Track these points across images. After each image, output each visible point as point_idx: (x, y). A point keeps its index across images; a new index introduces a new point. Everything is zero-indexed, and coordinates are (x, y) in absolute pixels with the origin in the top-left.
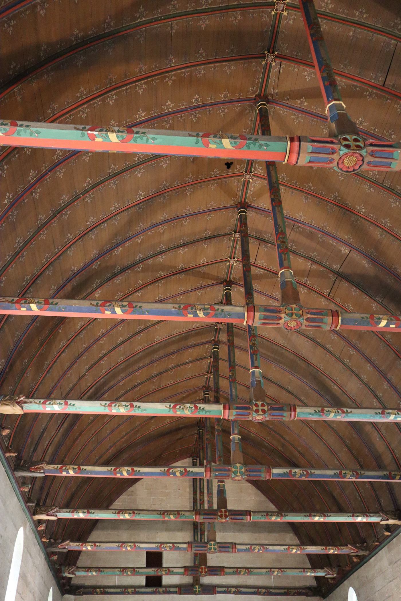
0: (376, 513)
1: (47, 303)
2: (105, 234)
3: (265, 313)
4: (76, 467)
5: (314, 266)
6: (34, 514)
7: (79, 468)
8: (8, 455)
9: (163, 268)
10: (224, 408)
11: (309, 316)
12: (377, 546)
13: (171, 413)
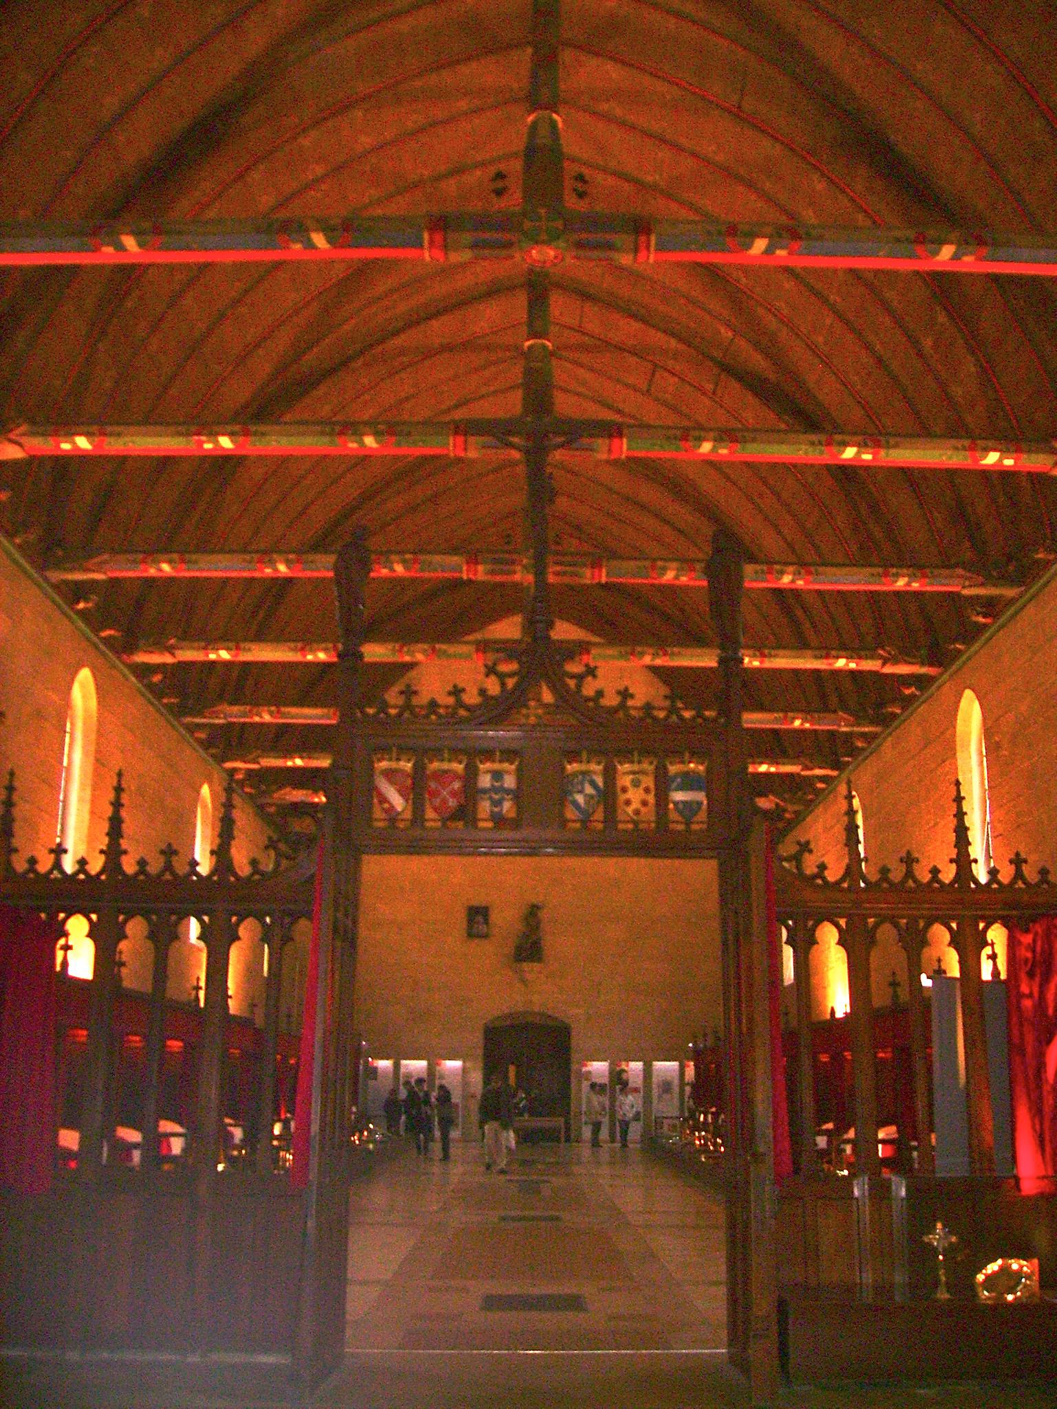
0: (794, 759)
1: (183, 561)
2: (282, 342)
3: (489, 567)
4: (273, 708)
5: (681, 347)
6: (224, 761)
7: (278, 712)
8: (165, 701)
9: (402, 352)
10: (477, 650)
11: (558, 568)
12: (811, 801)
13: (396, 658)
